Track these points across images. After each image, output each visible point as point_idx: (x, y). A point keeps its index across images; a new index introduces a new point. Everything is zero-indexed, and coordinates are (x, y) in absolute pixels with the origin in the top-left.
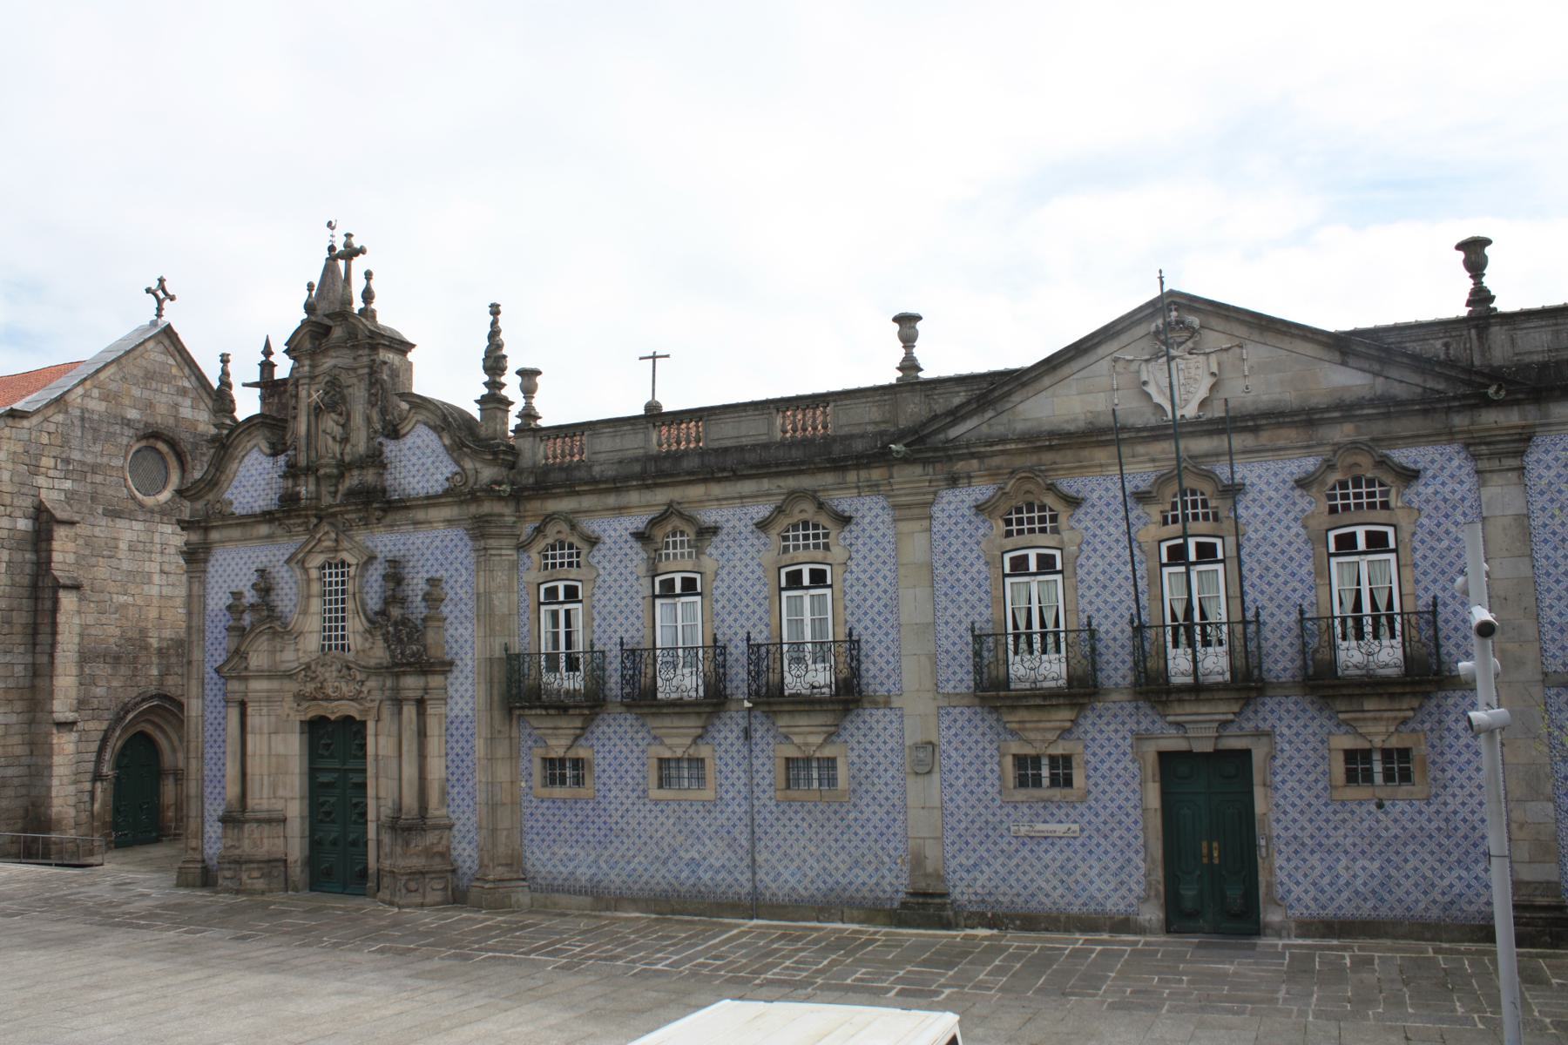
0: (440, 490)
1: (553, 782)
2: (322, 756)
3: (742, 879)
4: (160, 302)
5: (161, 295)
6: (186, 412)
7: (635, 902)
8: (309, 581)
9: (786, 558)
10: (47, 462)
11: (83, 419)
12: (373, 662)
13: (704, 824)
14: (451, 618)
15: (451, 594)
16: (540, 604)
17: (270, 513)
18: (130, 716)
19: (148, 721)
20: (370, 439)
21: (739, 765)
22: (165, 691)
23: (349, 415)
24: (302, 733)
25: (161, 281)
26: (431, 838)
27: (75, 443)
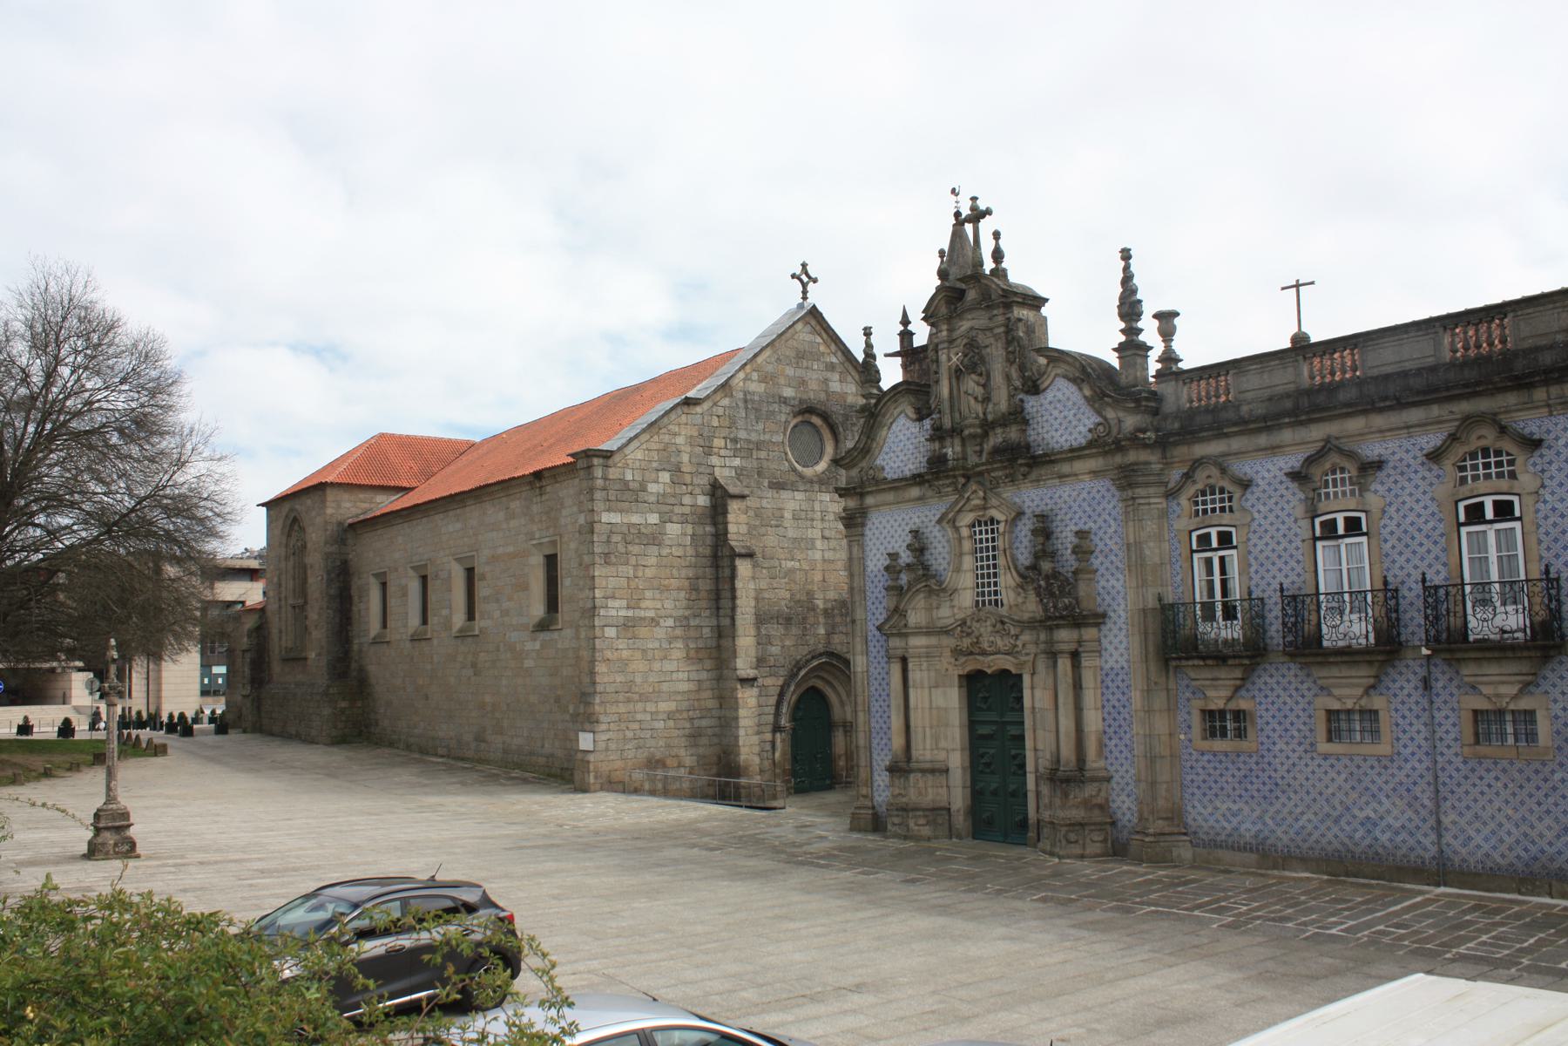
0: (1084, 442)
1: (1213, 735)
2: (980, 709)
3: (1427, 842)
4: (804, 285)
5: (805, 279)
6: (835, 386)
7: (1305, 861)
8: (960, 539)
9: (1464, 491)
10: (718, 442)
11: (746, 401)
12: (1026, 616)
13: (1379, 781)
14: (1102, 570)
15: (1101, 545)
16: (1192, 551)
17: (920, 475)
18: (802, 673)
19: (818, 677)
20: (1011, 396)
21: (1418, 717)
22: (832, 648)
23: (988, 376)
24: (960, 687)
25: (804, 266)
26: (1089, 790)
27: (740, 423)
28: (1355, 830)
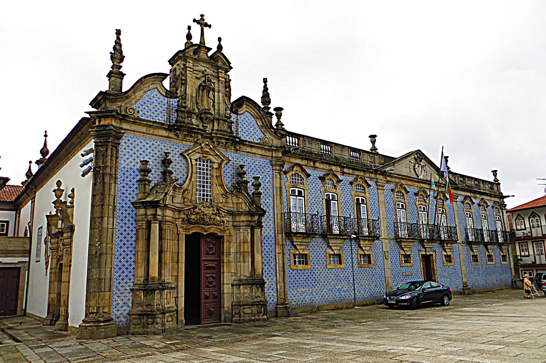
28: (336, 293)
